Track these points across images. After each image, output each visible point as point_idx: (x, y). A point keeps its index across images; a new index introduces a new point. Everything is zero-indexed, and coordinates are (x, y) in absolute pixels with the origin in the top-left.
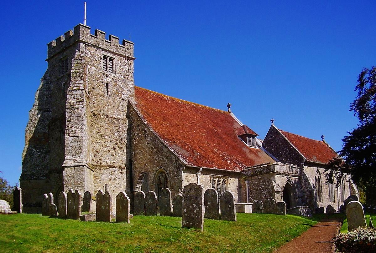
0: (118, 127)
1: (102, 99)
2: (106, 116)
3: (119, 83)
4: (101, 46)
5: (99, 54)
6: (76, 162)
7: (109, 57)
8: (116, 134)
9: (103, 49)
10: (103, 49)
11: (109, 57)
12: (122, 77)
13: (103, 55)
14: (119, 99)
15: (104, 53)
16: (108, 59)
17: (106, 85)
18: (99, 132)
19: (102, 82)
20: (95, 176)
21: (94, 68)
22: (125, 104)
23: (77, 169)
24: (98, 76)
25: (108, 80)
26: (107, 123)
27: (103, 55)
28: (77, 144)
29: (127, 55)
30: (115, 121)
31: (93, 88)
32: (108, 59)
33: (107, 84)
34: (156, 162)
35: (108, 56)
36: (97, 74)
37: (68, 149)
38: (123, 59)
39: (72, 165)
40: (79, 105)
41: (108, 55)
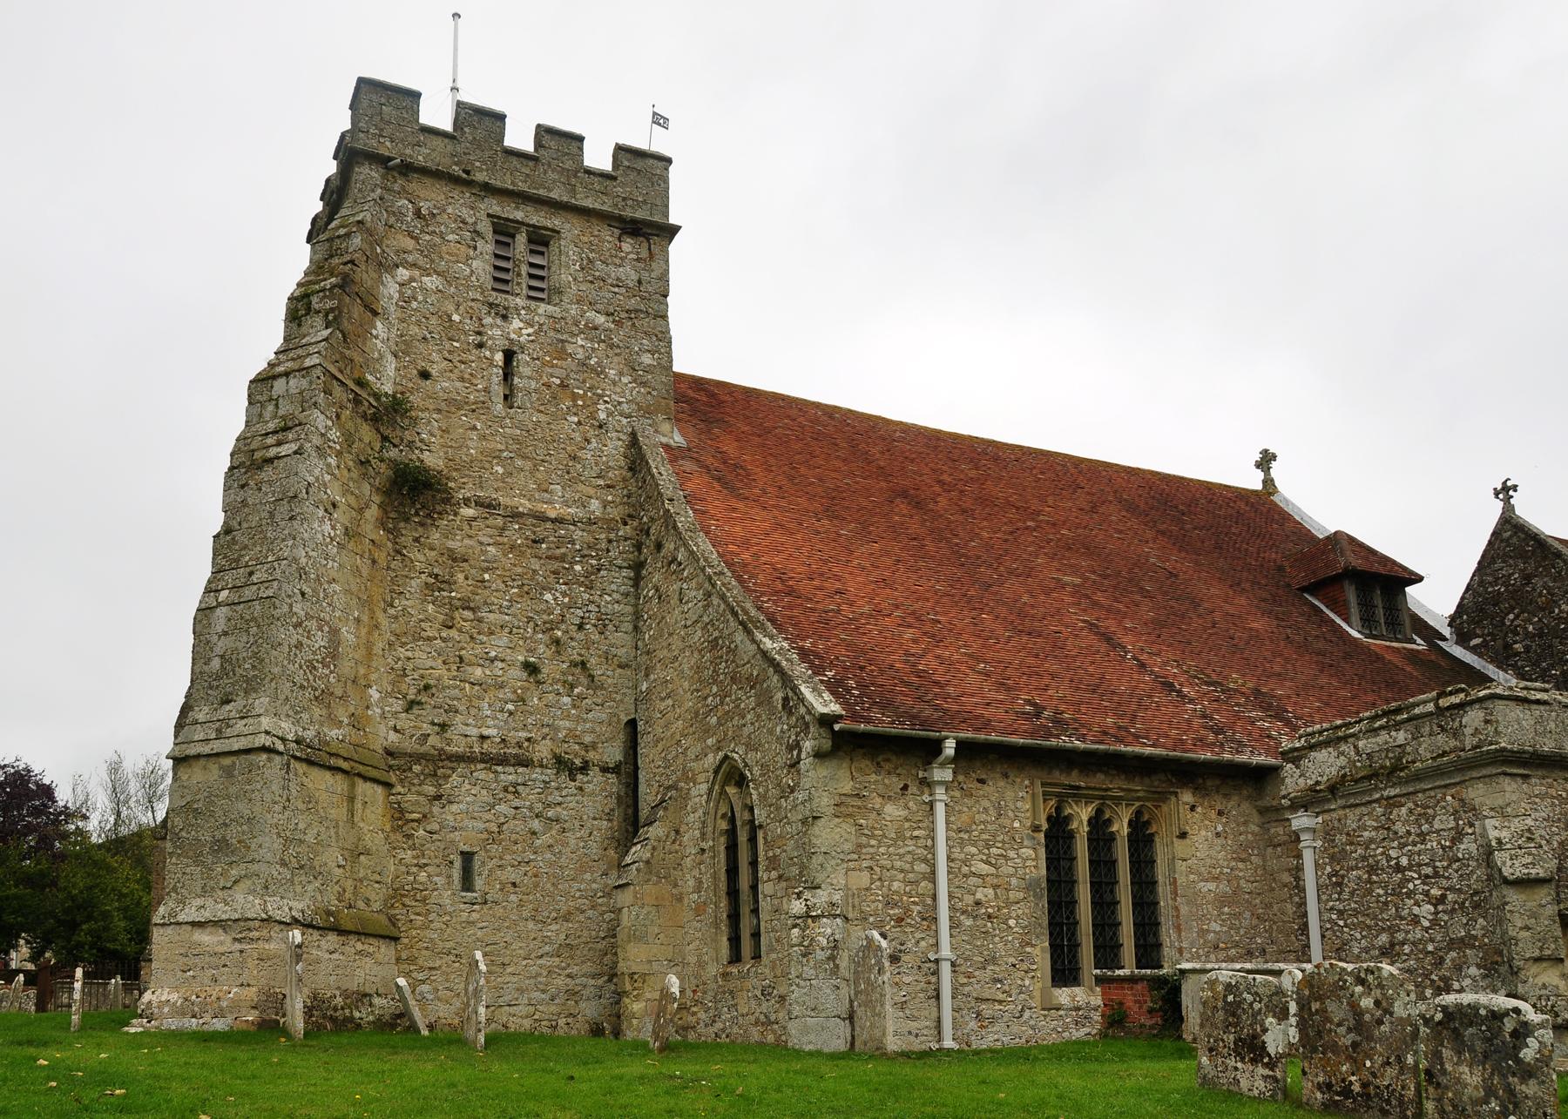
0: (562, 558)
1: (474, 428)
2: (488, 506)
3: (579, 345)
4: (480, 177)
5: (465, 213)
6: (229, 732)
7: (522, 223)
8: (548, 596)
9: (488, 189)
10: (488, 189)
11: (524, 229)
12: (601, 319)
13: (489, 215)
14: (579, 423)
15: (495, 206)
16: (521, 239)
17: (499, 357)
18: (439, 583)
19: (480, 346)
20: (402, 811)
21: (431, 282)
22: (614, 447)
23: (228, 772)
24: (456, 318)
25: (513, 336)
26: (496, 544)
27: (489, 215)
28: (245, 639)
29: (628, 213)
30: (543, 530)
31: (425, 375)
32: (521, 239)
33: (509, 355)
34: (714, 720)
35: (517, 222)
36: (451, 308)
37: (206, 668)
38: (608, 235)
39: (206, 749)
40: (279, 444)
41: (519, 215)
